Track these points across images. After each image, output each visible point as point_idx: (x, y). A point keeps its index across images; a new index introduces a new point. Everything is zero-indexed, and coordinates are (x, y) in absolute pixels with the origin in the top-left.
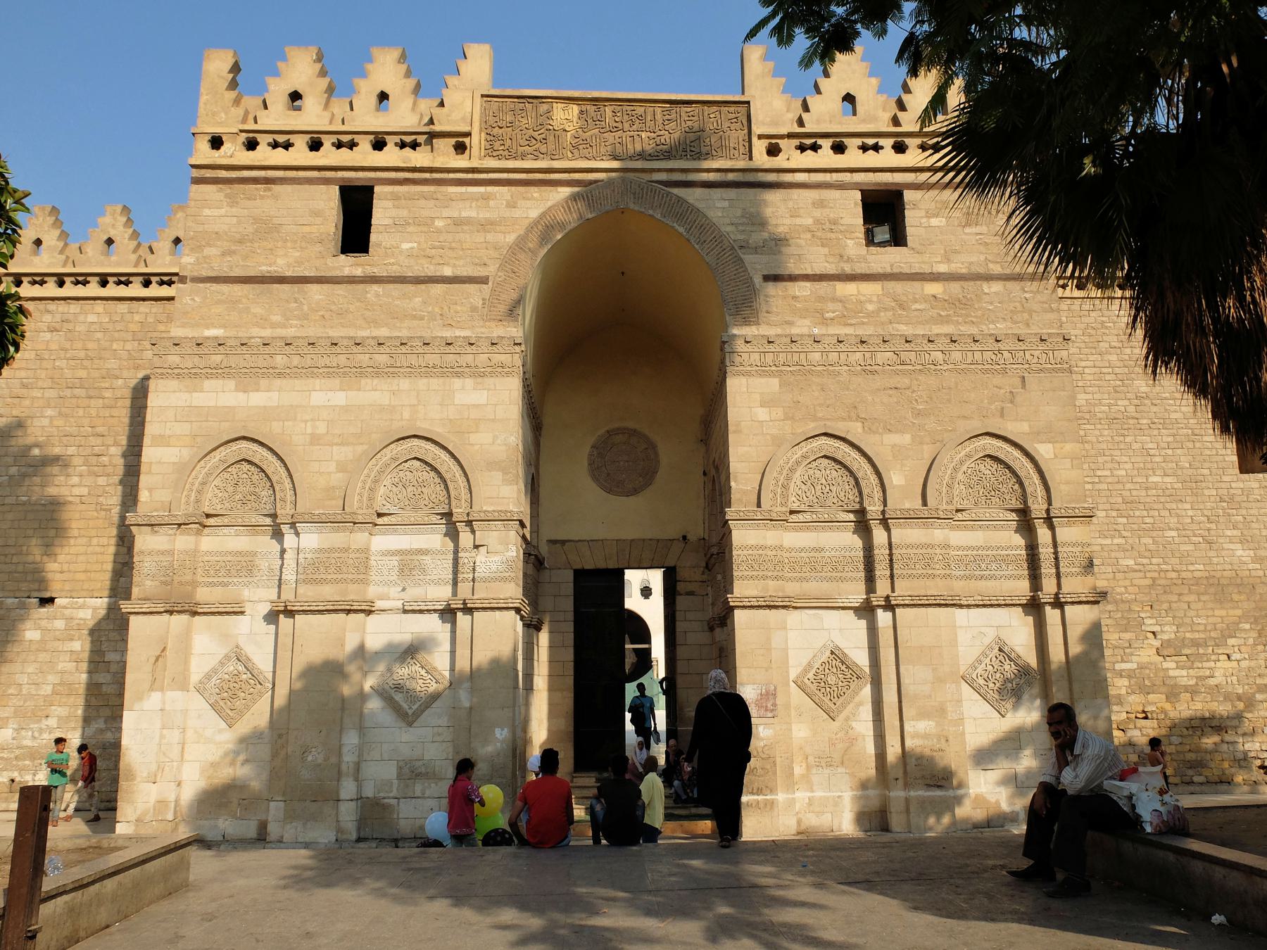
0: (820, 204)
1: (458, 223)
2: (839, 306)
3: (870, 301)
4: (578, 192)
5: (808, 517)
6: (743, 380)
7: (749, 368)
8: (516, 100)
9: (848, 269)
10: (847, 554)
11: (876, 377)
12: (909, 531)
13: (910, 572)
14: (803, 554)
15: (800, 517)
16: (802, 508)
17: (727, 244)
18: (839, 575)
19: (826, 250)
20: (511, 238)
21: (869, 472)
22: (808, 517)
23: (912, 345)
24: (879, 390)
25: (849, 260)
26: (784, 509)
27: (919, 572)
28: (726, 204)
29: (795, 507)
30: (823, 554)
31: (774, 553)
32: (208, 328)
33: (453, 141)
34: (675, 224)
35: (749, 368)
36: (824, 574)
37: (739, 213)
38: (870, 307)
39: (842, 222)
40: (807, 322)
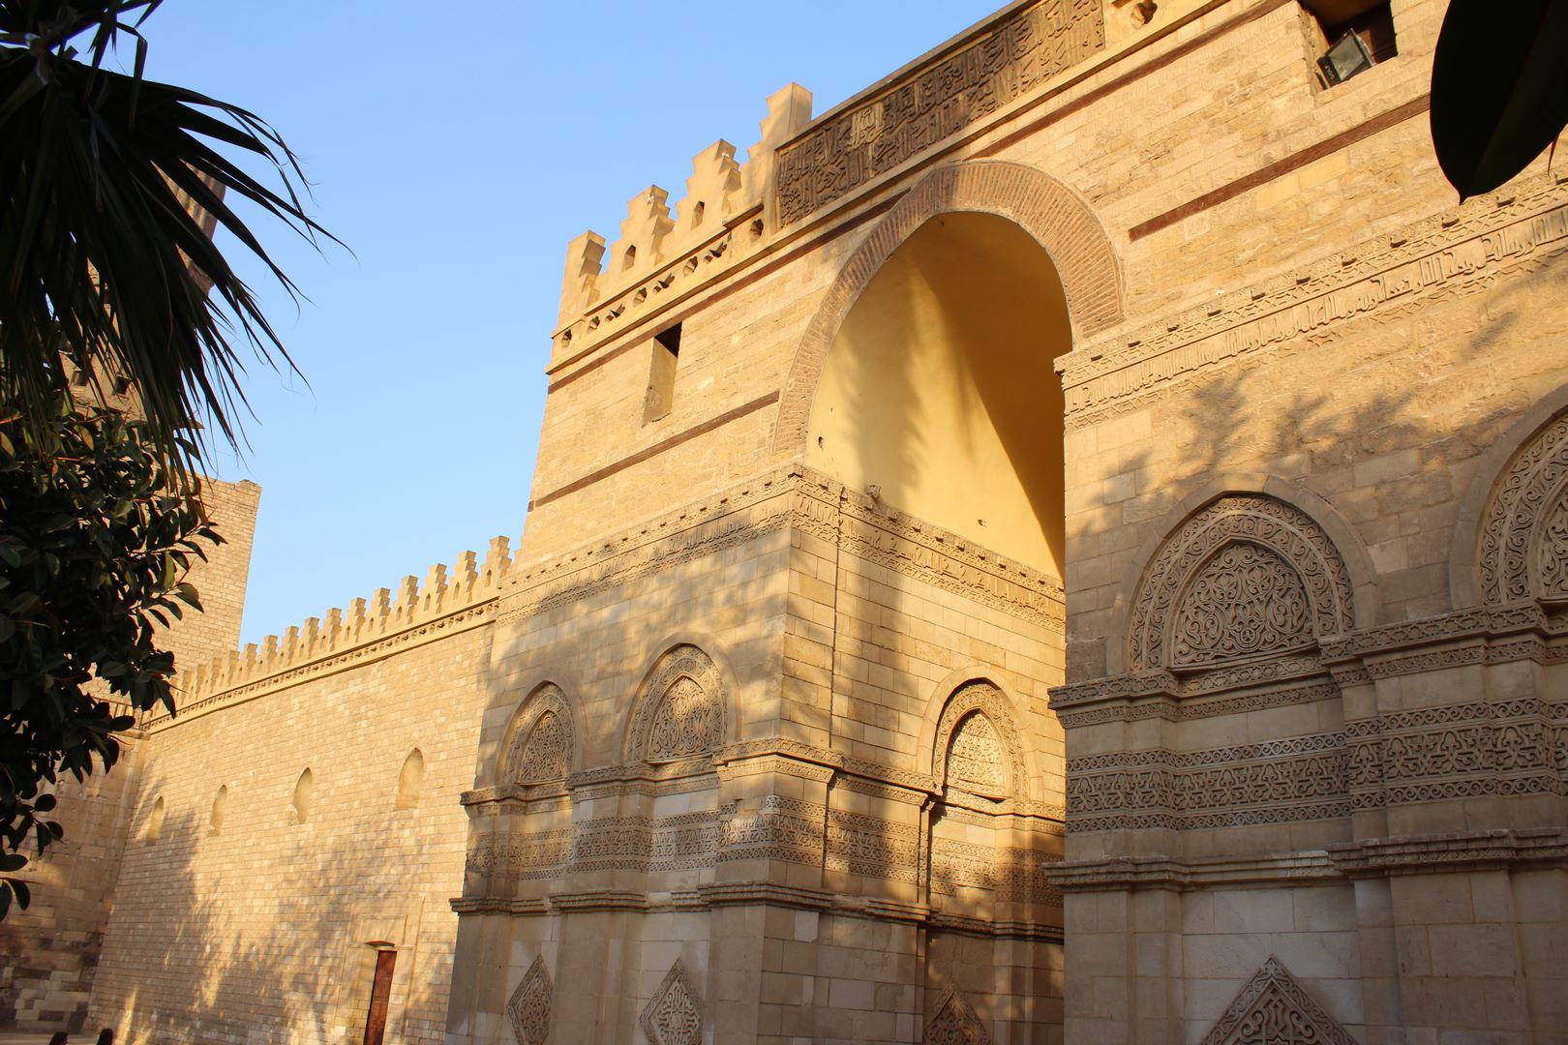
0: (1225, 60)
1: (753, 329)
2: (1265, 231)
3: (1325, 196)
4: (881, 222)
5: (1217, 682)
6: (1090, 431)
7: (1101, 406)
8: (813, 135)
9: (1277, 153)
10: (1308, 754)
11: (1337, 344)
12: (1417, 681)
13: (1423, 782)
14: (1218, 765)
15: (1208, 685)
16: (1209, 662)
17: (1072, 203)
18: (1291, 804)
19: (1237, 137)
20: (803, 325)
21: (1320, 557)
22: (1217, 682)
23: (1409, 249)
24: (1343, 370)
25: (1280, 134)
26: (1154, 671)
27: (1448, 779)
28: (1072, 138)
29: (1184, 664)
30: (1257, 760)
31: (1144, 767)
32: (542, 556)
33: (748, 225)
34: (1000, 208)
35: (1101, 406)
36: (1259, 806)
37: (1089, 143)
38: (1325, 208)
39: (1262, 73)
40: (1205, 284)
